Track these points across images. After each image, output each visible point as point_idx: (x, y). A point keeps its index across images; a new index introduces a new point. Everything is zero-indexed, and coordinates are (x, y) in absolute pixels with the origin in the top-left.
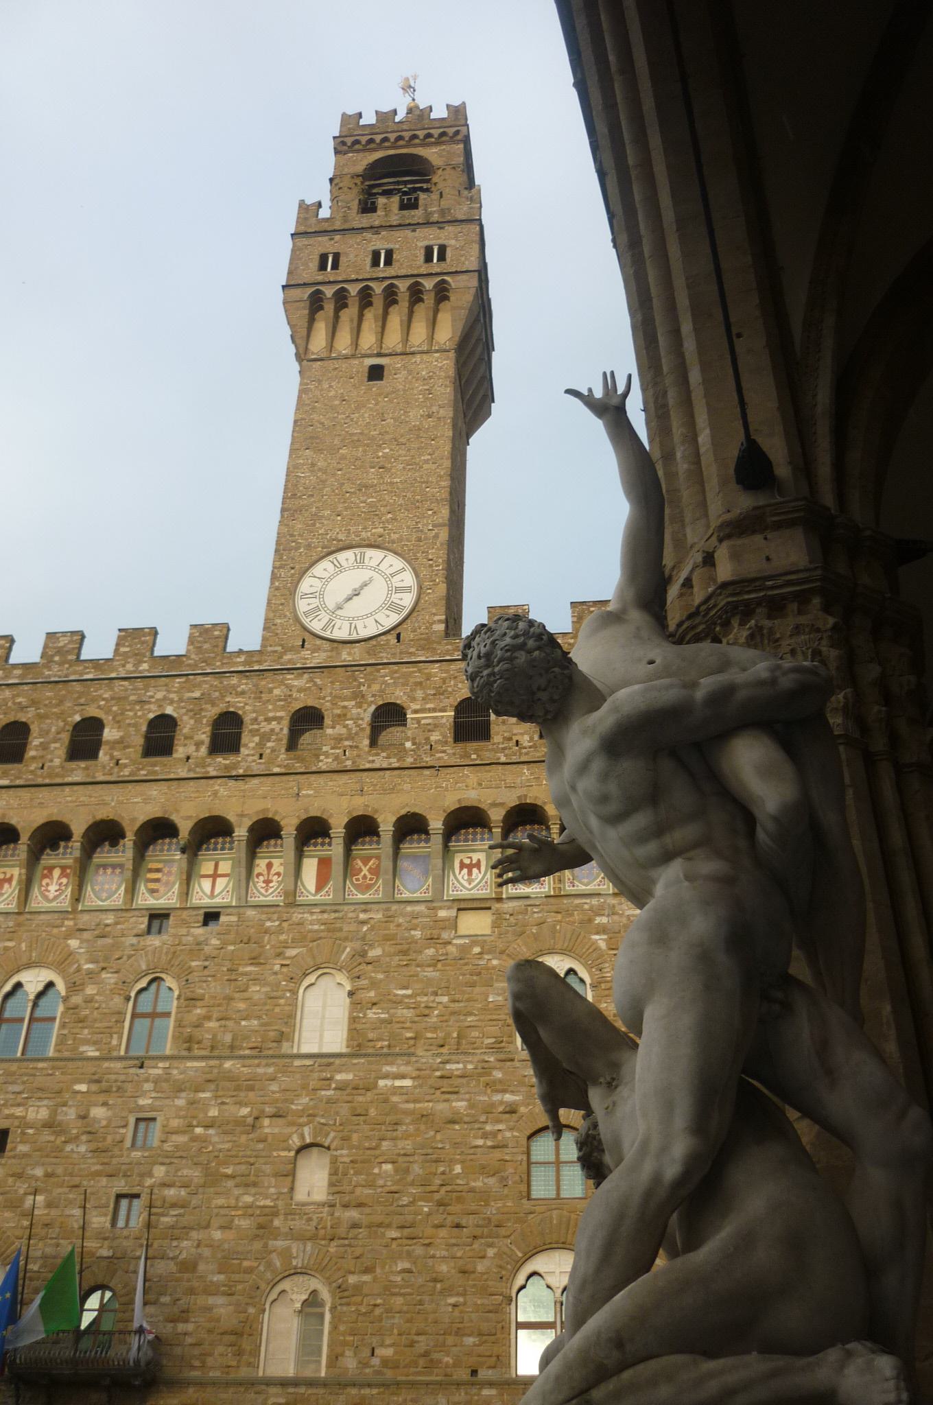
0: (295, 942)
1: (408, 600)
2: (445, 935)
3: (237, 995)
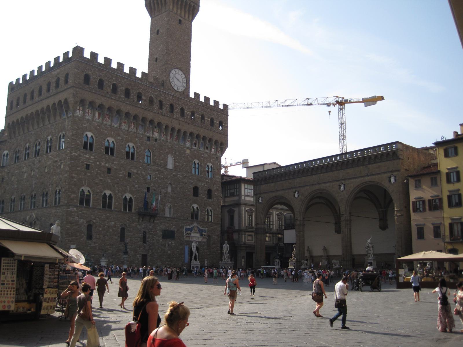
1: (185, 85)
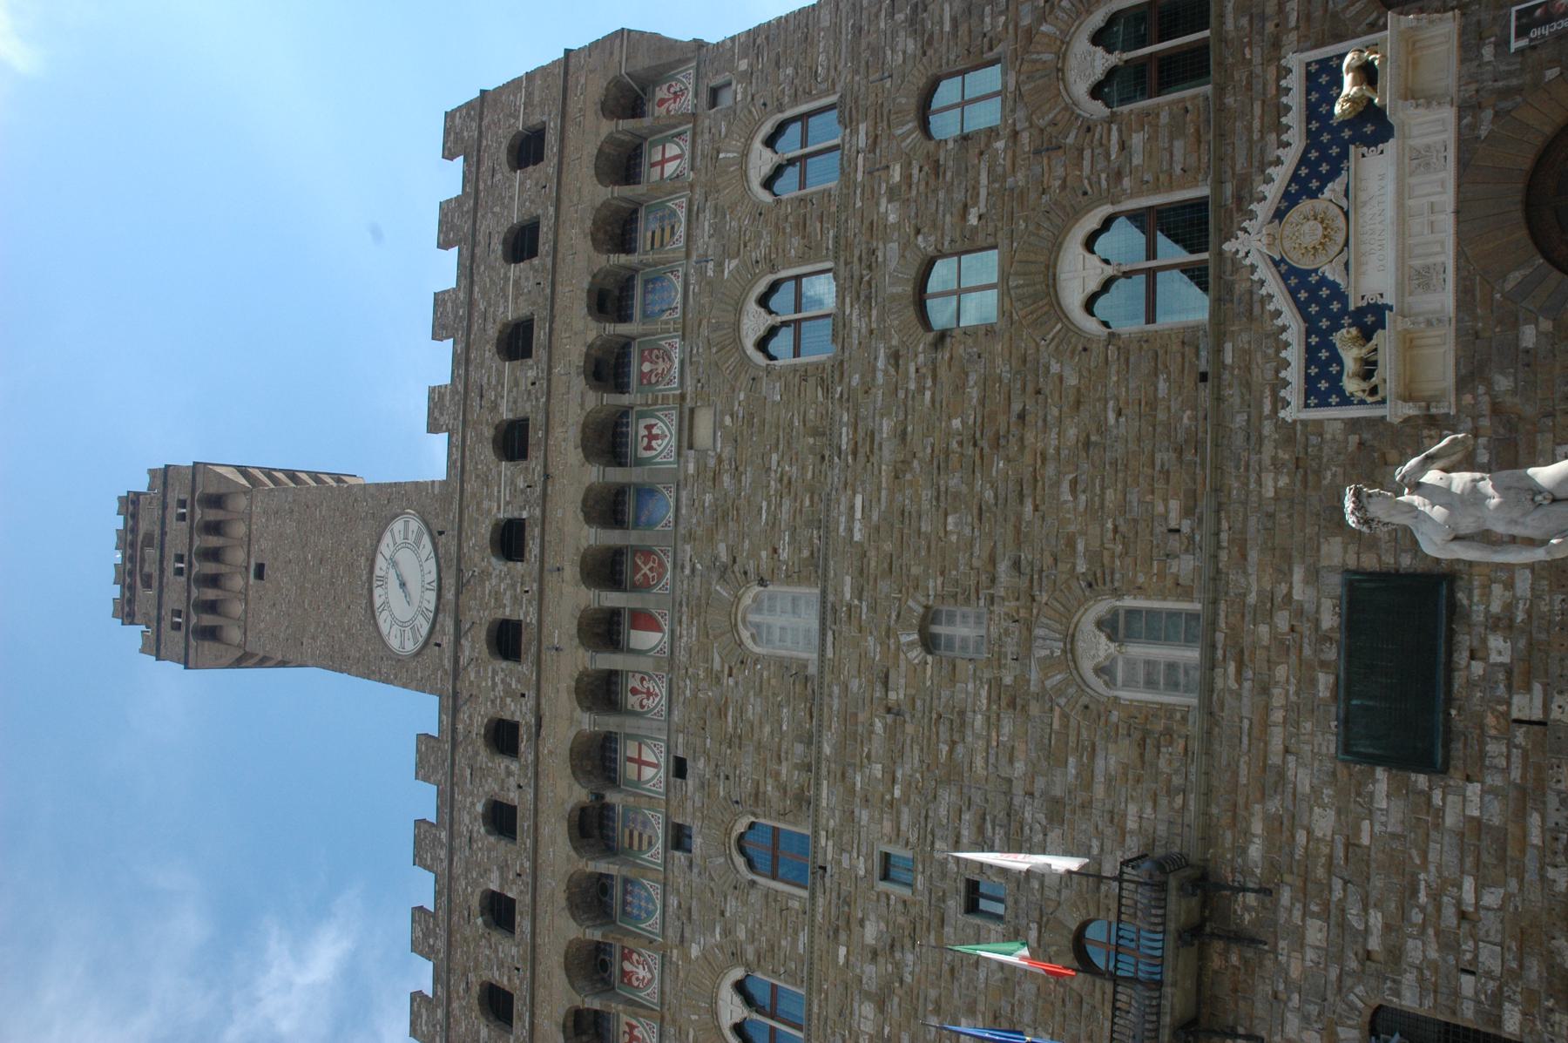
0: (708, 660)
1: (415, 525)
2: (712, 462)
3: (756, 737)
